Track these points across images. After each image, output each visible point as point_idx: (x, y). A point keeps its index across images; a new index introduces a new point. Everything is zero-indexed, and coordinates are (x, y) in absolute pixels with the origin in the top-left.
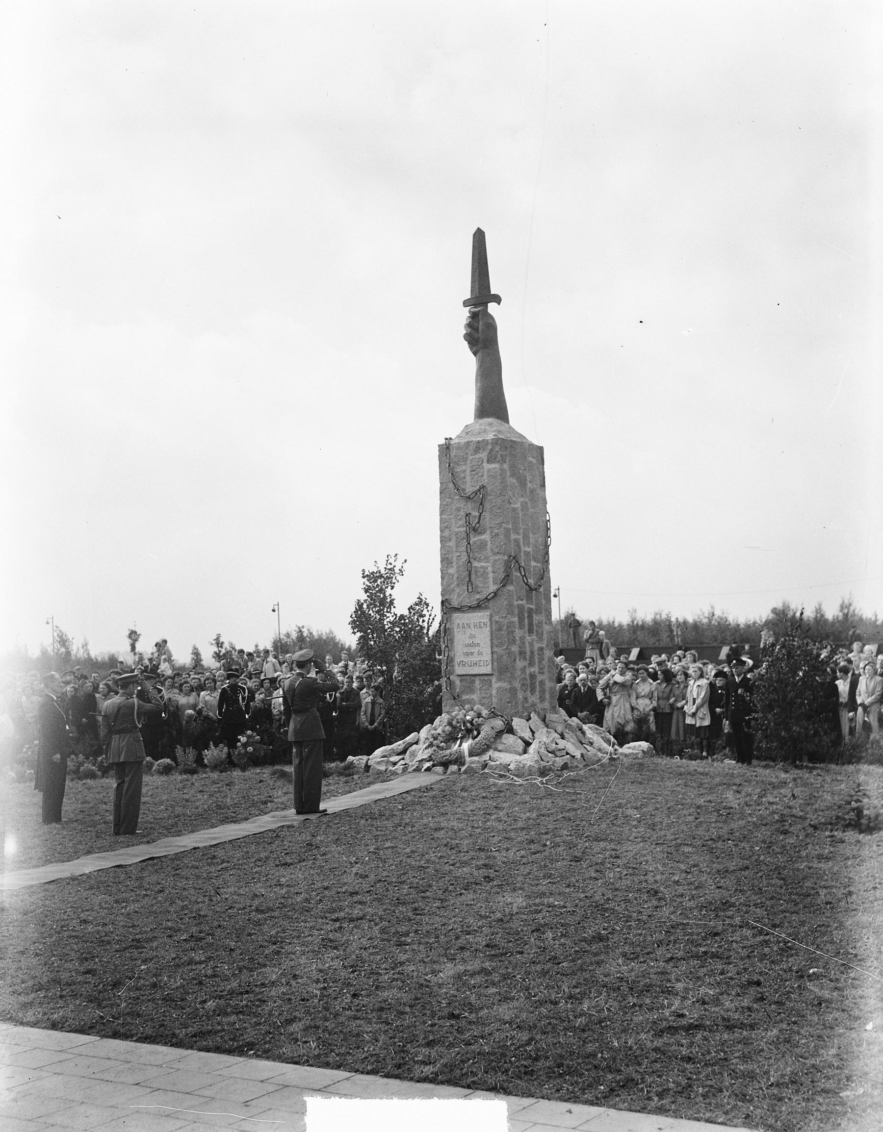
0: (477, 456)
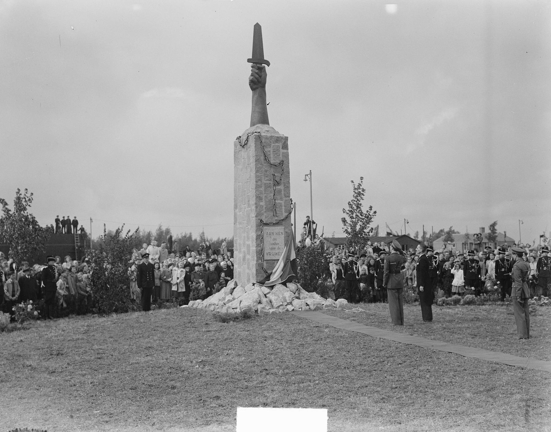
0: (277, 144)
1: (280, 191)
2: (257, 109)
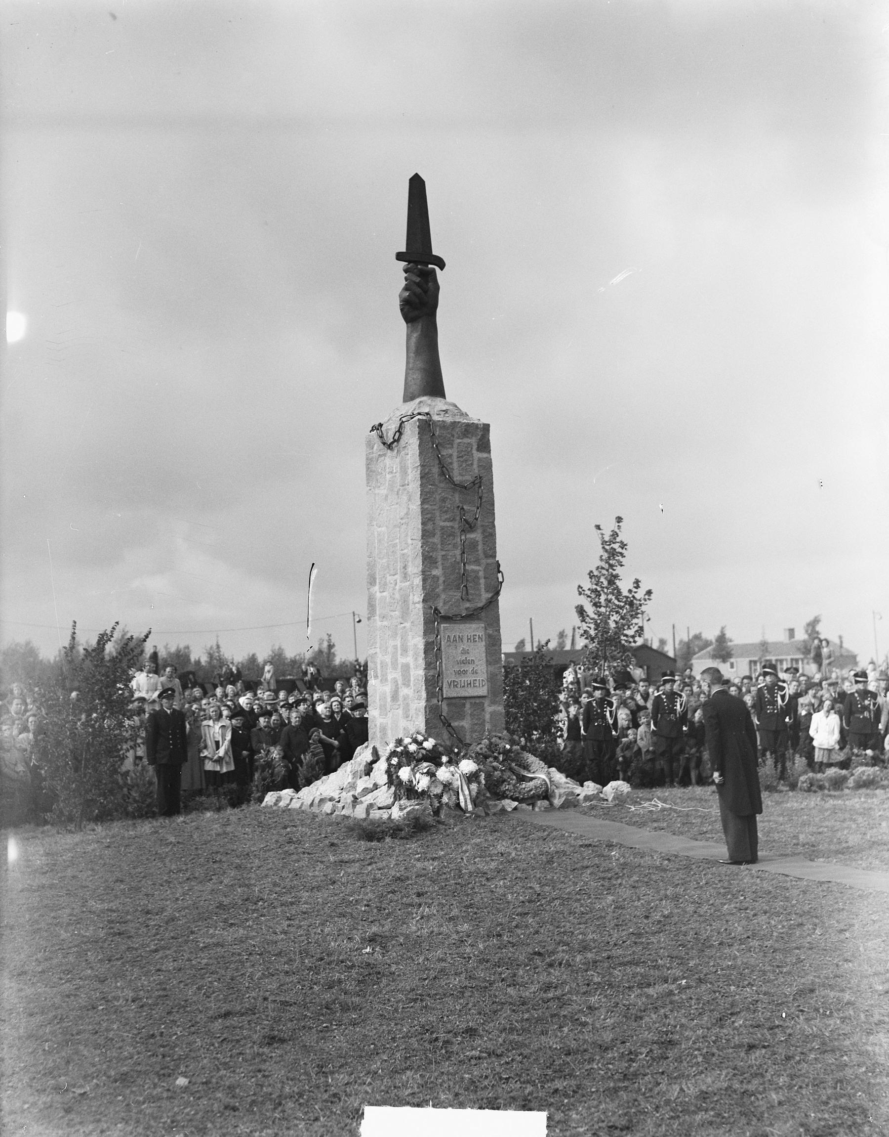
0: (466, 440)
2: (420, 364)
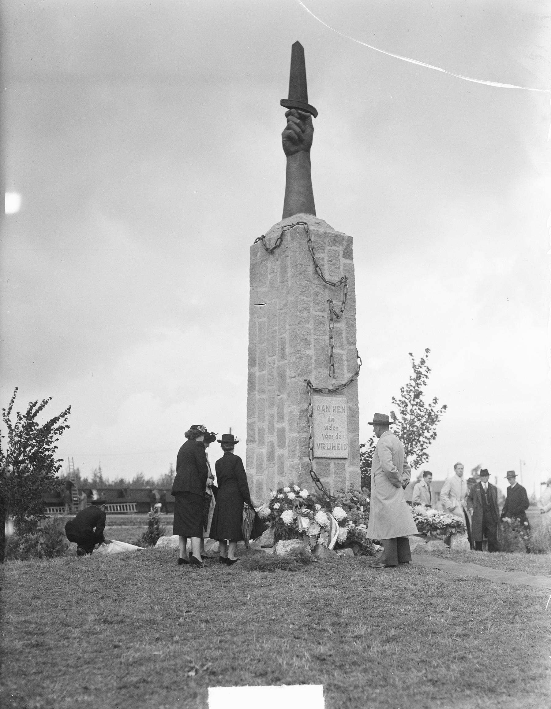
0: (334, 248)
1: (339, 333)
